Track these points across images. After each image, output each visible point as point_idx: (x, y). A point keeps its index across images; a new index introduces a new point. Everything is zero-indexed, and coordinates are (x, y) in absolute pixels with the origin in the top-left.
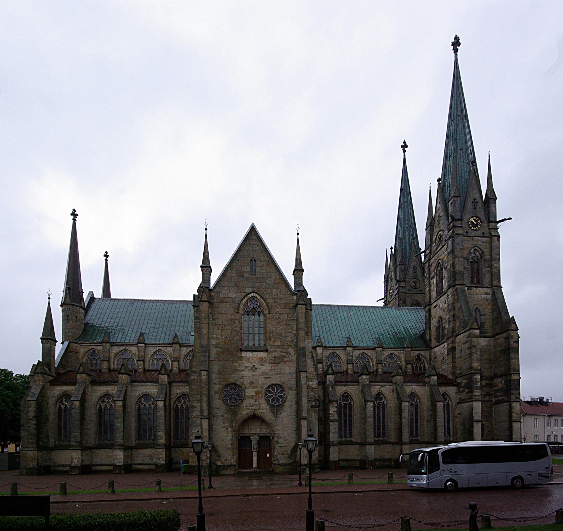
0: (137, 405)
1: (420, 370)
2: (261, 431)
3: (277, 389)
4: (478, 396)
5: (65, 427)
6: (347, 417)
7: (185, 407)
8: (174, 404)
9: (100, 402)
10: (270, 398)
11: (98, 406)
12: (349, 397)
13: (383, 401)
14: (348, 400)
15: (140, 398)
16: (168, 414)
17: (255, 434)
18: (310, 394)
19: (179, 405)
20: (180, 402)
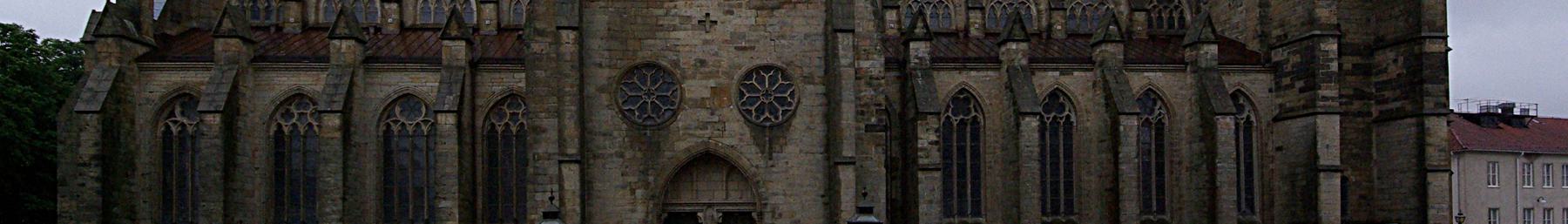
0: (382, 124)
1: (1171, 26)
2: (727, 198)
3: (773, 81)
4: (1333, 99)
5: (182, 187)
6: (965, 157)
7: (514, 129)
8: (485, 121)
9: (278, 116)
10: (751, 105)
11: (274, 128)
12: (972, 102)
13: (1067, 113)
14: (969, 109)
15: (389, 105)
16: (467, 149)
17: (710, 205)
18: (863, 94)
19: (497, 124)
20: (502, 116)
